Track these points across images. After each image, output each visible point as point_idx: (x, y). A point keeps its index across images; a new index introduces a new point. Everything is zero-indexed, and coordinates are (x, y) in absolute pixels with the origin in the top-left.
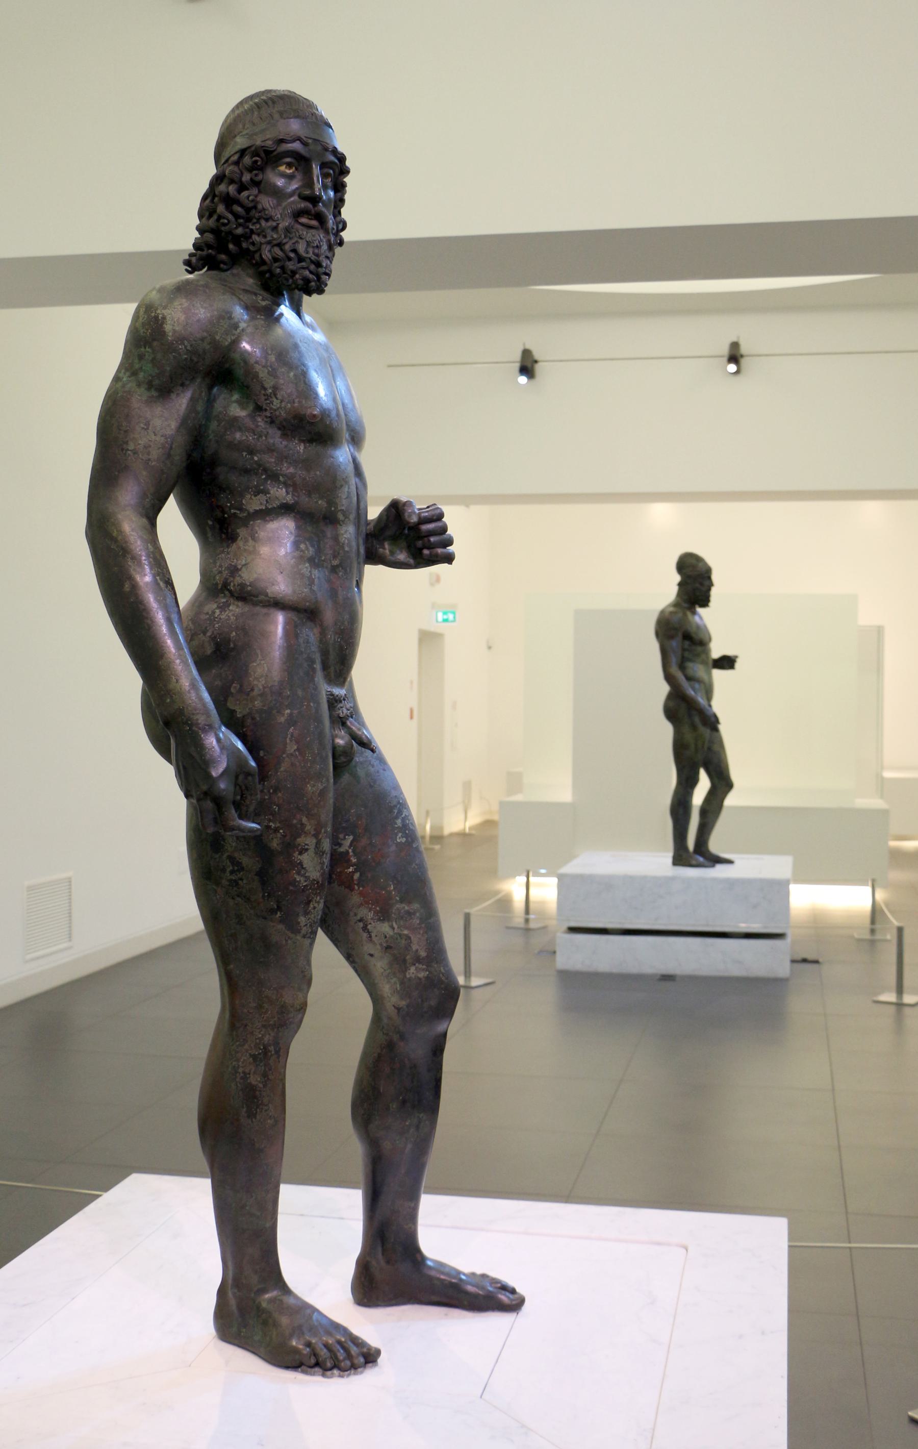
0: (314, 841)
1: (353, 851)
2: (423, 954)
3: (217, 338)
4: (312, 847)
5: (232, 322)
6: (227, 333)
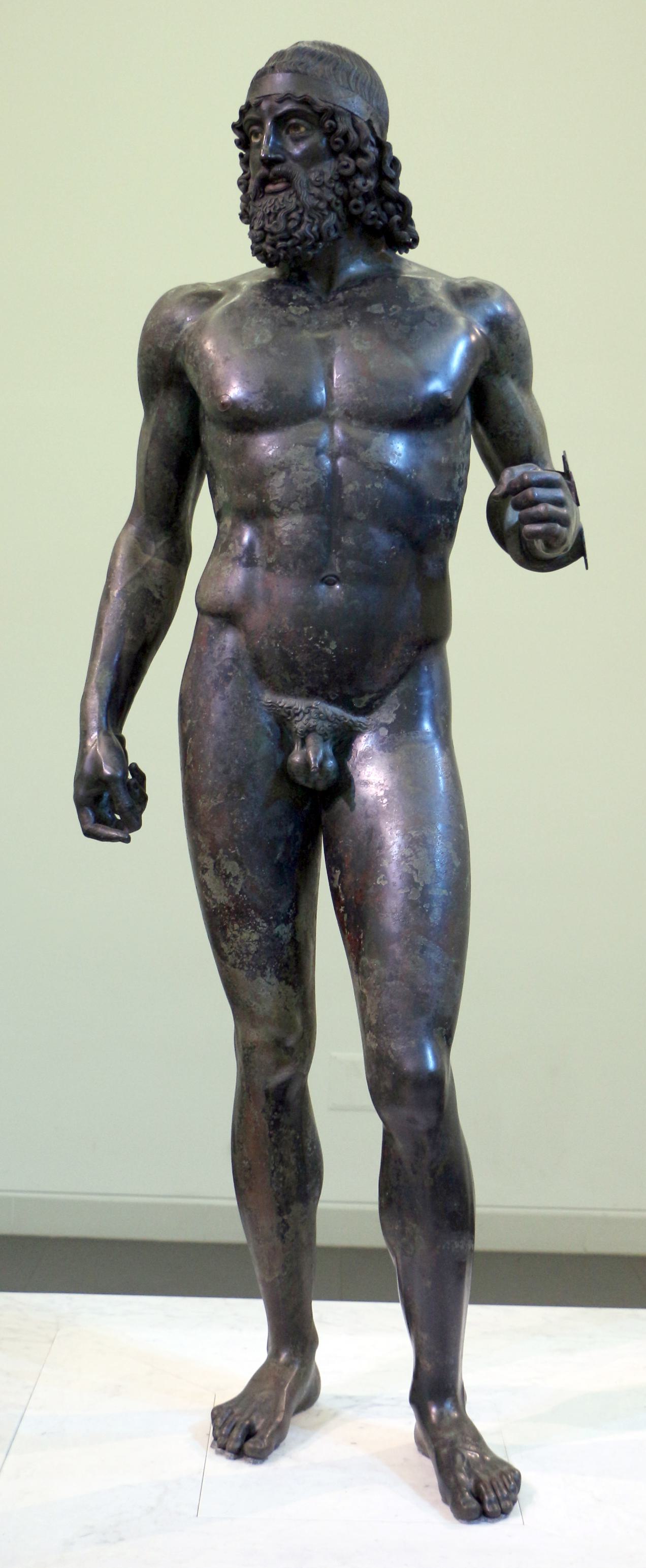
0: (212, 861)
1: (342, 888)
2: (374, 1021)
3: (160, 346)
4: (211, 867)
5: (174, 326)
6: (169, 338)
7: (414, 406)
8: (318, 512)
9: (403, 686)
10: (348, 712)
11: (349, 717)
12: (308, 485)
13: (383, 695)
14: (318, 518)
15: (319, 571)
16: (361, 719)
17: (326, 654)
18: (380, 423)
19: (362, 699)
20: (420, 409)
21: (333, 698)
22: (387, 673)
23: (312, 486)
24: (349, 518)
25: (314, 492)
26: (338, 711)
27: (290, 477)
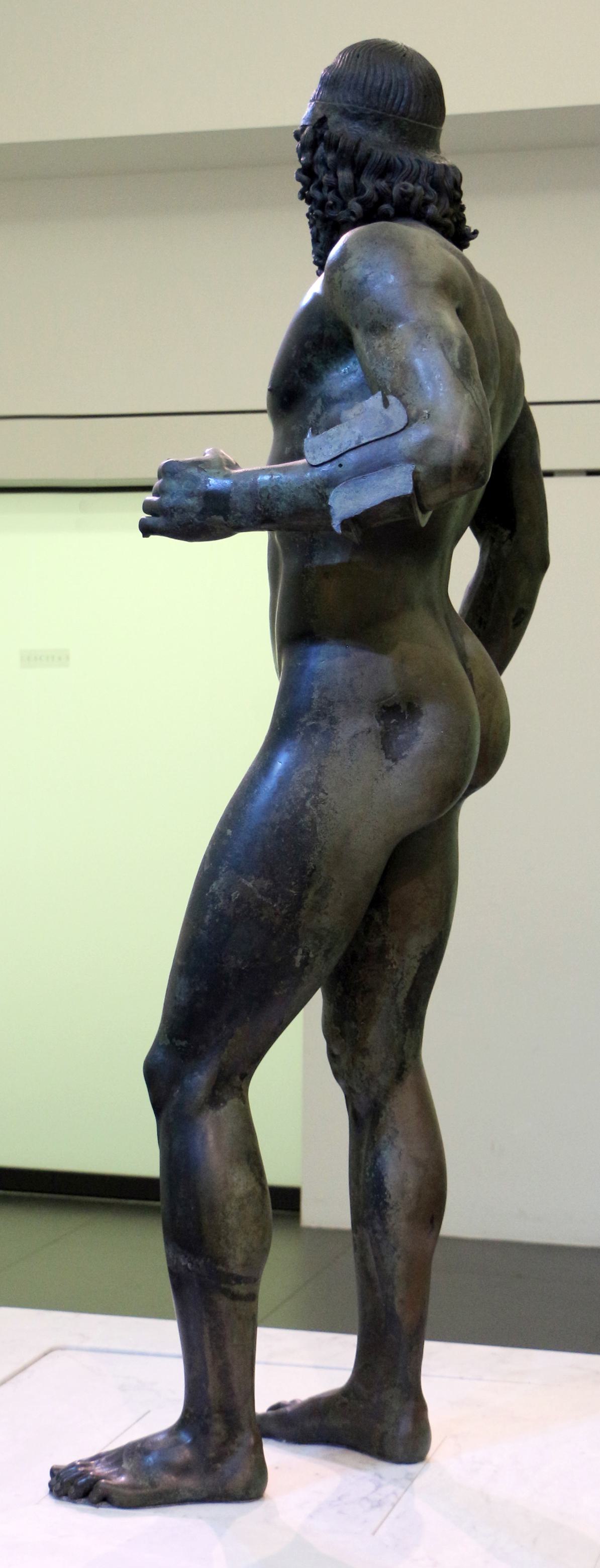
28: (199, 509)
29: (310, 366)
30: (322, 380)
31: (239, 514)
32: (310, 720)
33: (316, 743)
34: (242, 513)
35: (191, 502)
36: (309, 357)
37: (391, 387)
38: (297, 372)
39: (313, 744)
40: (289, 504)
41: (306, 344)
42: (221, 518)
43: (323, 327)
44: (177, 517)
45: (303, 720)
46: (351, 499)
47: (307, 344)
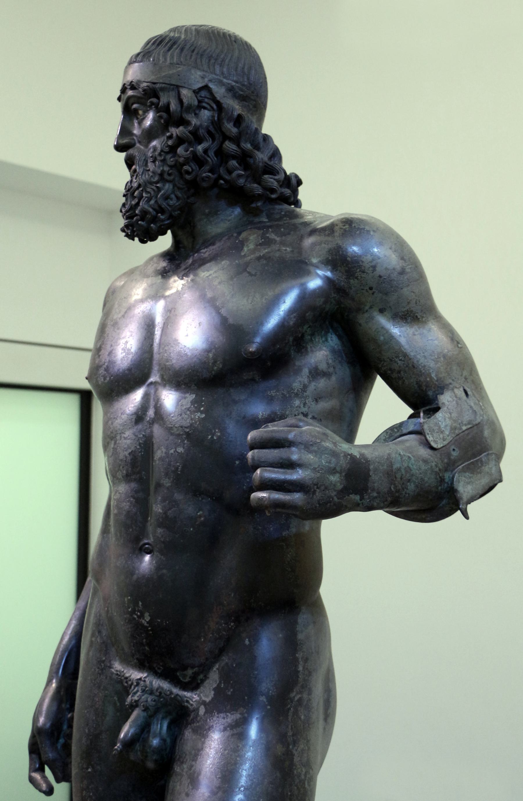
7: (215, 362)
8: (135, 480)
9: (225, 659)
10: (176, 686)
11: (176, 691)
12: (126, 453)
13: (205, 669)
14: (133, 485)
15: (137, 539)
16: (188, 694)
17: (142, 625)
18: (186, 384)
19: (185, 672)
20: (221, 366)
21: (159, 671)
22: (206, 646)
23: (129, 454)
24: (159, 485)
25: (131, 460)
26: (165, 685)
27: (116, 446)
28: (339, 487)
29: (303, 336)
30: (307, 352)
31: (375, 494)
32: (297, 693)
33: (302, 717)
34: (378, 493)
35: (334, 478)
36: (305, 327)
37: (436, 376)
38: (291, 339)
39: (300, 718)
40: (417, 486)
41: (307, 314)
42: (357, 497)
43: (325, 302)
44: (318, 495)
45: (292, 695)
46: (468, 483)
47: (309, 315)
